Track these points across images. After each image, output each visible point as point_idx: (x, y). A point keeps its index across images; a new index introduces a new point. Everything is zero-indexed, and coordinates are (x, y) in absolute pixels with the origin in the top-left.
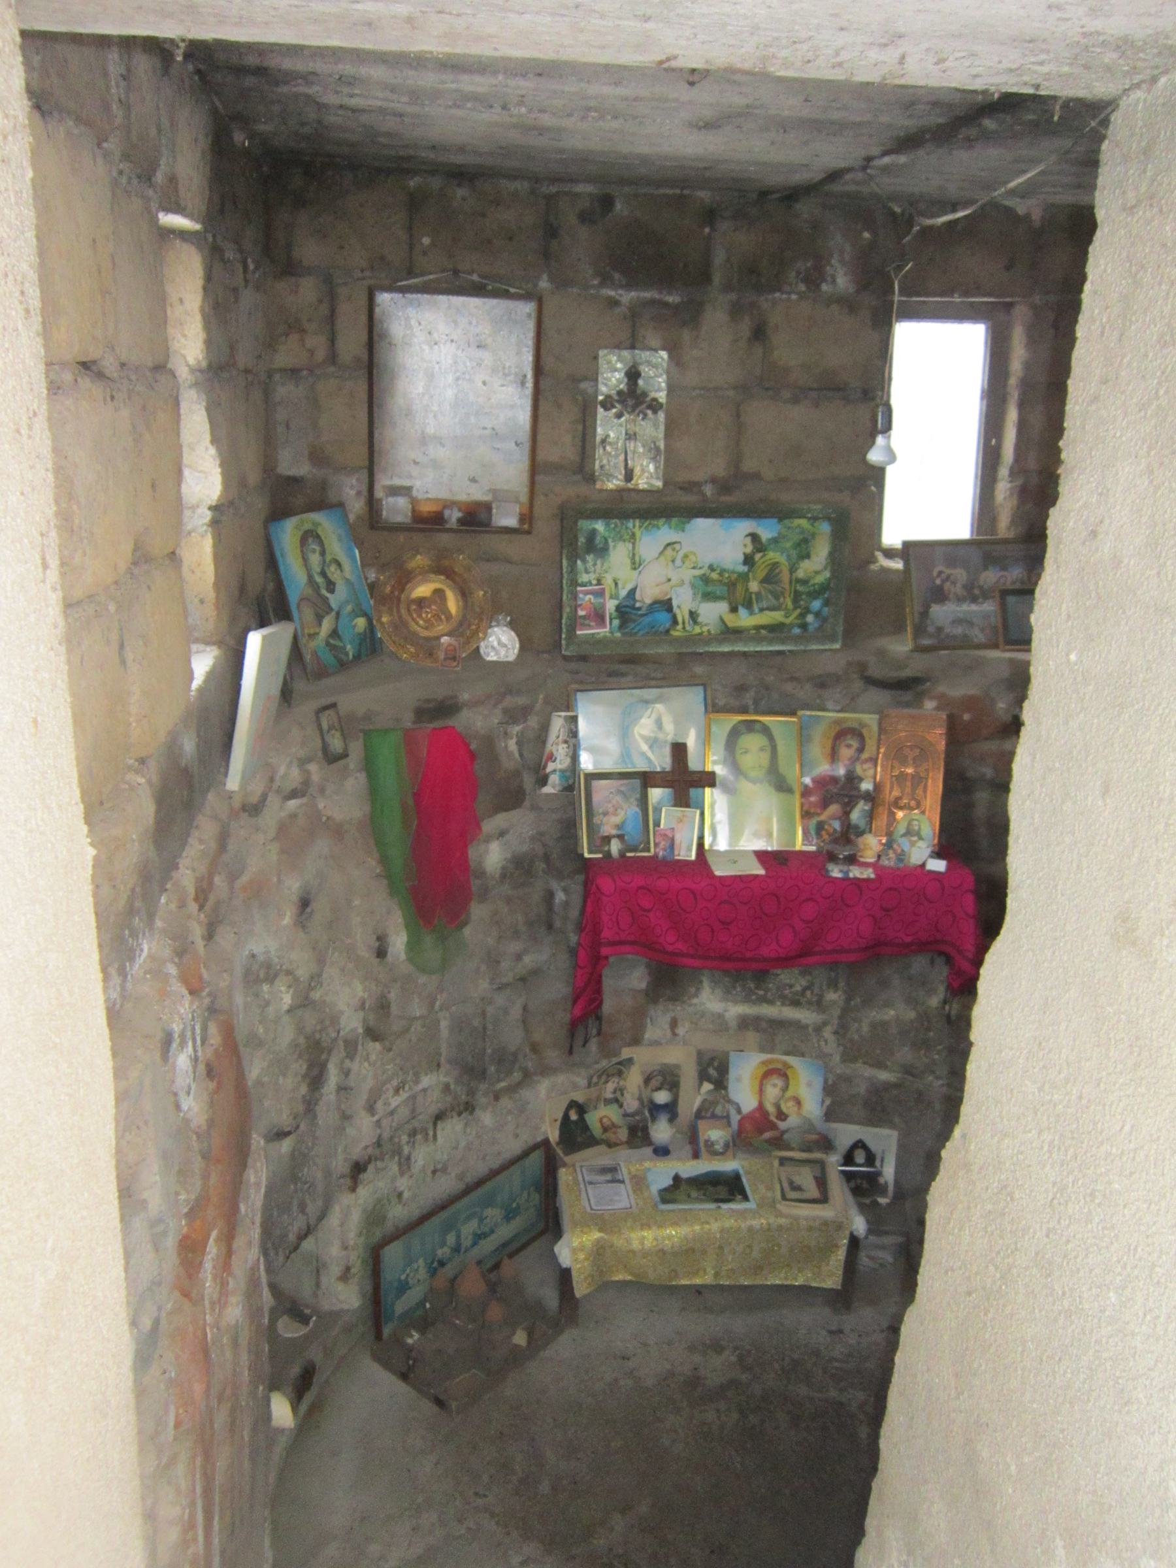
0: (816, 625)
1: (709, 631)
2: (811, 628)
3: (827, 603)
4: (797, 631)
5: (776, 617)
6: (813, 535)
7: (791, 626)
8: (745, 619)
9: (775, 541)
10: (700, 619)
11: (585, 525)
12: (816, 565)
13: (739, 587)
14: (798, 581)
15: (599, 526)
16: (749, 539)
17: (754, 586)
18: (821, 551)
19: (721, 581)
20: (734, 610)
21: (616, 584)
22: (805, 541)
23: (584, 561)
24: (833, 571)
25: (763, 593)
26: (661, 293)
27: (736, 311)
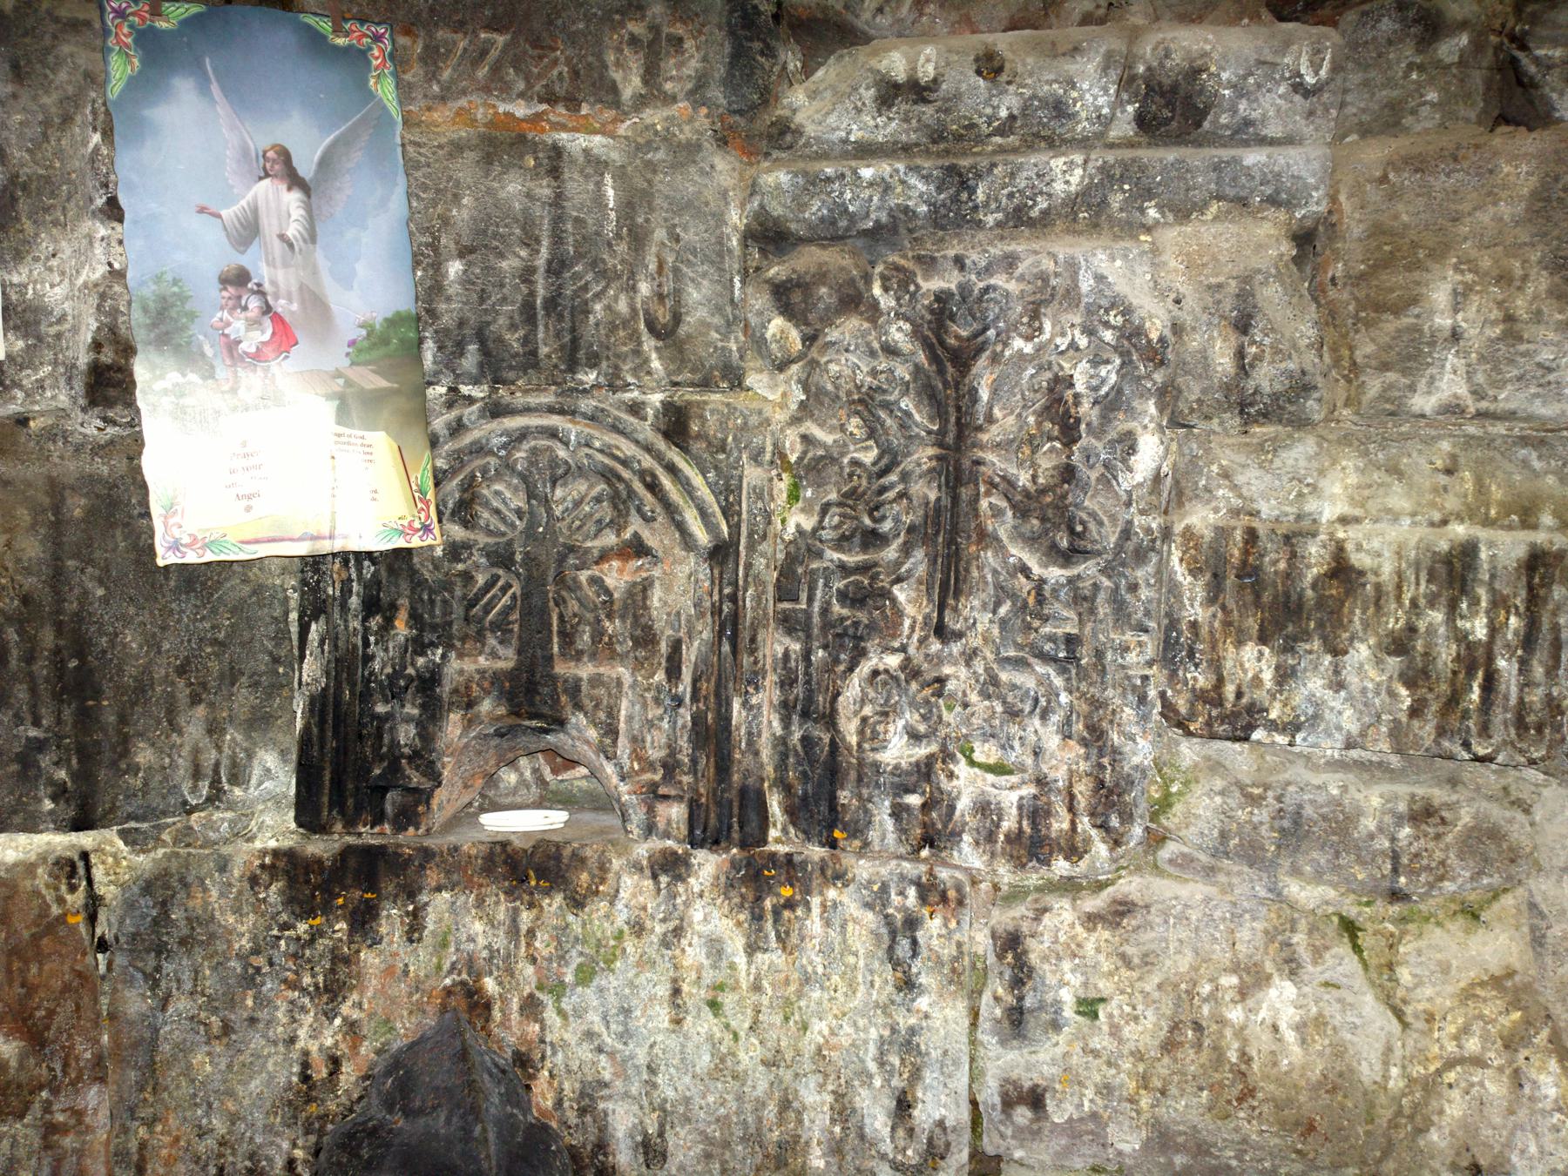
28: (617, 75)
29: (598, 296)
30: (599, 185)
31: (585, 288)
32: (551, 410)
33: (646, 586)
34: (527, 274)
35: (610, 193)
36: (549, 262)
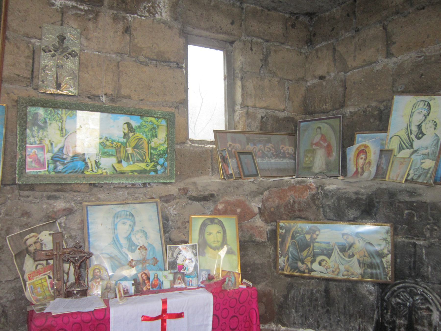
0: (162, 171)
1: (106, 172)
2: (159, 172)
3: (166, 160)
4: (153, 173)
5: (143, 166)
6: (158, 126)
7: (150, 171)
8: (125, 167)
9: (139, 127)
10: (101, 166)
11: (31, 110)
12: (161, 140)
13: (122, 150)
14: (152, 148)
15: (41, 111)
16: (126, 125)
17: (130, 150)
18: (162, 135)
19: (112, 146)
20: (120, 162)
21: (52, 144)
22: (154, 128)
23: (32, 131)
24: (169, 144)
25: (135, 154)
26: (77, 4)
27: (116, 19)
28: (425, 233)
29: (422, 267)
30: (422, 250)
31: (420, 266)
32: (414, 283)
33: (430, 315)
34: (410, 263)
35: (424, 252)
36: (414, 261)
